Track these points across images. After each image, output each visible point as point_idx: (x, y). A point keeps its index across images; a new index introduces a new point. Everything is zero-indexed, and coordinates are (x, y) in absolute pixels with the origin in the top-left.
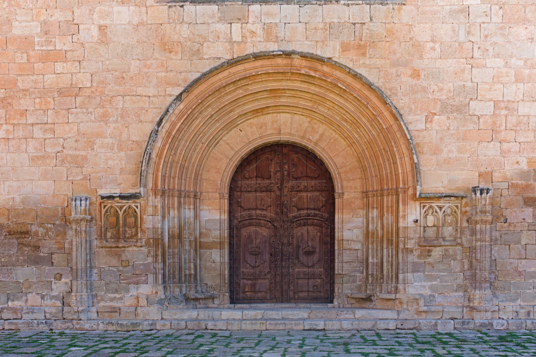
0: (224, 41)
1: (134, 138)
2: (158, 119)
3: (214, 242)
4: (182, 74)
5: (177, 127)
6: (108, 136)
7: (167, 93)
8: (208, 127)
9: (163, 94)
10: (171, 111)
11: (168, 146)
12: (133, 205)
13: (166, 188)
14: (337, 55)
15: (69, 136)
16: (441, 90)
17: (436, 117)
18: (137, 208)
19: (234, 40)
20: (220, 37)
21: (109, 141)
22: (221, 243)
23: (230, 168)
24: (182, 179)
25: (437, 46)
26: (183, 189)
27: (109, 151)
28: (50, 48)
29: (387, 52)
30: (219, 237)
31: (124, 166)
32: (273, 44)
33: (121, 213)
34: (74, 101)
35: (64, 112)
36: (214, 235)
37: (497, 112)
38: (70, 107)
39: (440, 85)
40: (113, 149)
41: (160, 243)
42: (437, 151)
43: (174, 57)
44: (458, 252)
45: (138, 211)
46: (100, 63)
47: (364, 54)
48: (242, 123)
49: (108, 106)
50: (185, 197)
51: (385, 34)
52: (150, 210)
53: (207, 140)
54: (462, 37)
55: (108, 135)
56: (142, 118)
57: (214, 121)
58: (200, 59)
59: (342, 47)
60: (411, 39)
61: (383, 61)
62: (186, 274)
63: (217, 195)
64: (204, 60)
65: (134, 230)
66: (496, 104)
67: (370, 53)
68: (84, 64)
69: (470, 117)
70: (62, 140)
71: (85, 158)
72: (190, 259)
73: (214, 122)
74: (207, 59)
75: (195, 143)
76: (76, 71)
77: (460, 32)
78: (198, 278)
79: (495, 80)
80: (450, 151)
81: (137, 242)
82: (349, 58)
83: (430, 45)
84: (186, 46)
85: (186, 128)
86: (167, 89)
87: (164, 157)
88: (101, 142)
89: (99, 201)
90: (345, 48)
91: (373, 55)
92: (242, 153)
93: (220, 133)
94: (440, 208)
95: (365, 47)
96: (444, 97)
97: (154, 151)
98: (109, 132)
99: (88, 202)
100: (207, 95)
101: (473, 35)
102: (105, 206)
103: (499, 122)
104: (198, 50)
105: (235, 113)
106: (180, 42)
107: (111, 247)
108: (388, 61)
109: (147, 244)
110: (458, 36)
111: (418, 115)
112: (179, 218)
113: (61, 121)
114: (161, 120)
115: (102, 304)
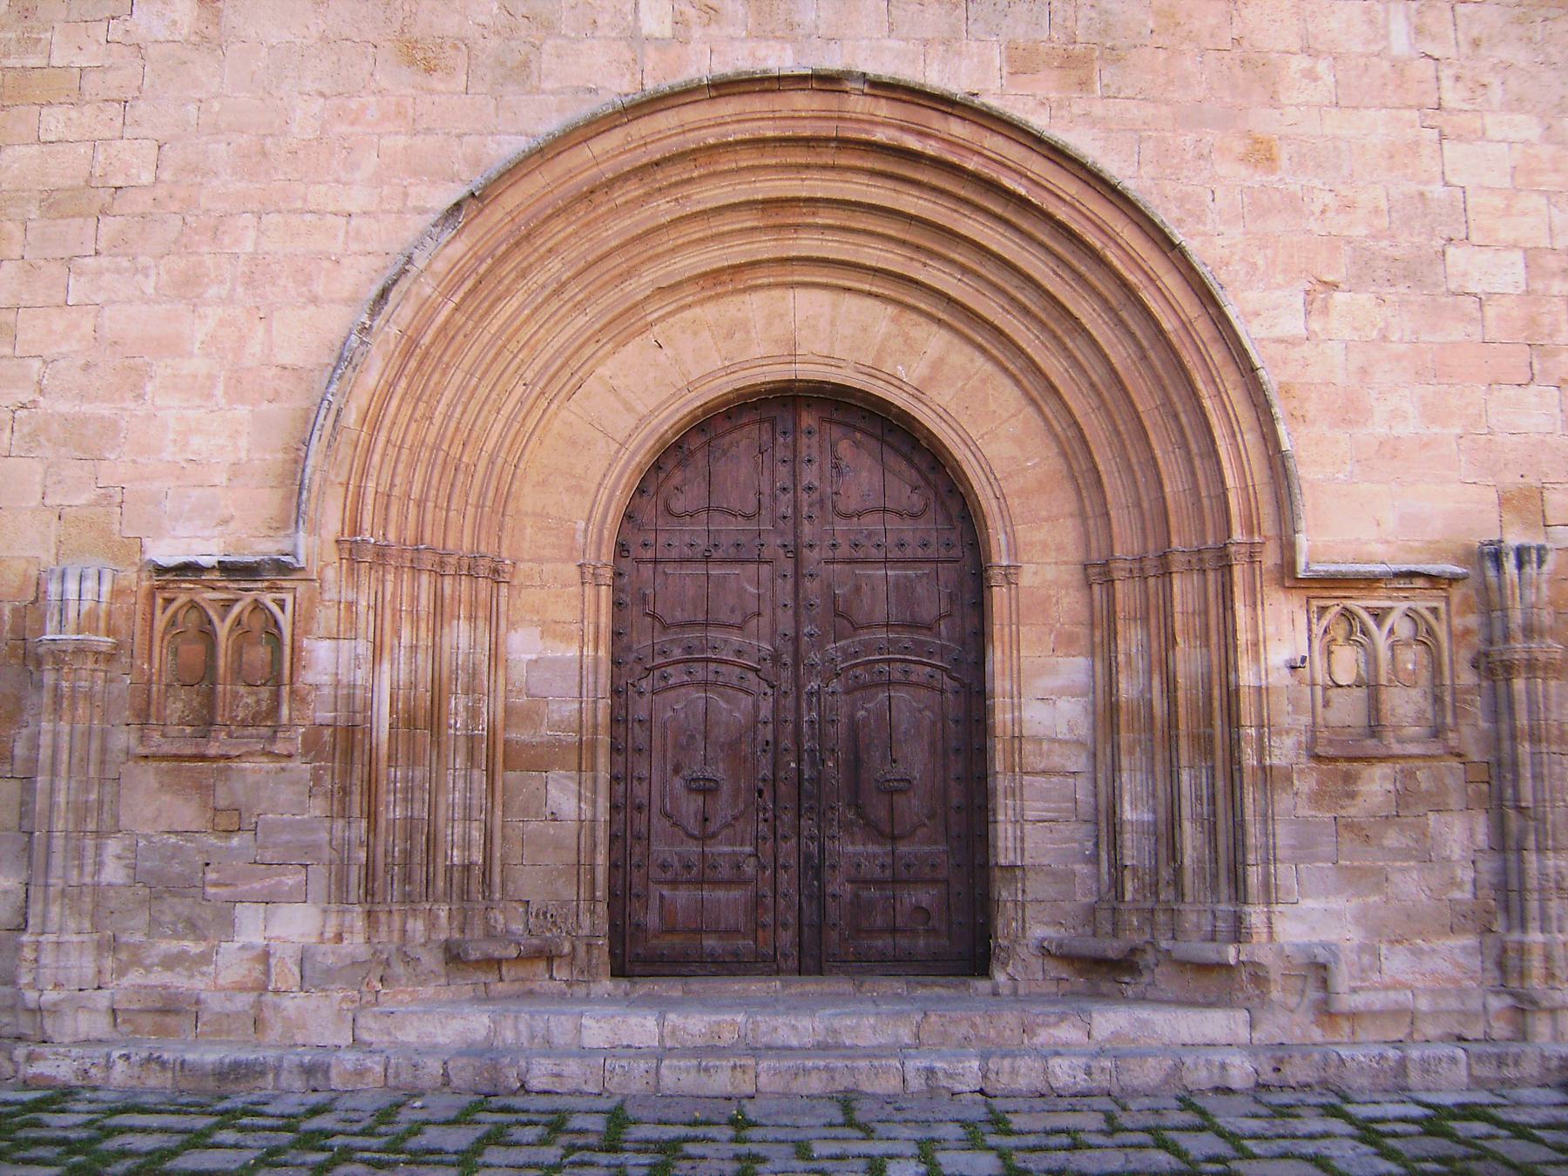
0: (613, 35)
1: (286, 358)
2: (375, 290)
3: (554, 745)
4: (465, 139)
5: (440, 320)
6: (196, 351)
7: (411, 203)
8: (547, 326)
9: (397, 205)
10: (420, 262)
11: (403, 383)
12: (268, 599)
13: (392, 537)
14: (994, 86)
15: (64, 349)
16: (1349, 206)
17: (1339, 297)
18: (283, 609)
19: (645, 32)
20: (600, 22)
21: (198, 365)
22: (584, 750)
23: (621, 476)
24: (448, 510)
25: (1322, 67)
26: (450, 545)
27: (197, 402)
28: (32, 61)
29: (1161, 80)
30: (576, 725)
31: (243, 455)
32: (778, 47)
33: (223, 630)
34: (92, 232)
35: (55, 269)
36: (556, 717)
37: (1539, 285)
38: (78, 251)
39: (1343, 190)
40: (210, 396)
41: (357, 743)
42: (1350, 412)
43: (441, 87)
44: (1449, 781)
45: (285, 620)
46: (192, 108)
47: (1084, 85)
48: (663, 318)
49: (205, 249)
50: (457, 575)
51: (1151, 24)
52: (326, 616)
53: (540, 374)
54: (1400, 41)
55: (197, 345)
56: (319, 289)
57: (570, 304)
58: (529, 93)
59: (1010, 60)
60: (1237, 41)
61: (1149, 110)
62: (453, 865)
63: (572, 571)
64: (542, 97)
65: (265, 693)
66: (1532, 257)
67: (1105, 81)
68: (142, 108)
69: (1451, 299)
70: (37, 364)
71: (110, 428)
72: (468, 807)
73: (570, 311)
74: (553, 93)
75: (501, 383)
76: (108, 135)
77: (1393, 27)
78: (497, 879)
79: (1521, 180)
80: (1396, 415)
81: (273, 739)
82: (1034, 96)
83: (1302, 62)
84: (483, 51)
85: (471, 324)
86: (412, 190)
87: (387, 422)
88: (169, 370)
89: (146, 584)
90: (1021, 63)
91: (1113, 88)
92: (661, 424)
93: (587, 352)
94: (1379, 616)
95: (1086, 61)
96: (1360, 231)
97: (353, 405)
98: (200, 336)
99: (106, 588)
100: (549, 211)
101: (1434, 38)
102: (169, 601)
103: (1547, 319)
104: (526, 64)
105: (643, 281)
106: (462, 40)
107: (178, 758)
108: (1164, 109)
109: (312, 745)
110: (1386, 37)
111: (1279, 287)
112: (436, 649)
113: (40, 301)
114: (384, 294)
115: (134, 977)
